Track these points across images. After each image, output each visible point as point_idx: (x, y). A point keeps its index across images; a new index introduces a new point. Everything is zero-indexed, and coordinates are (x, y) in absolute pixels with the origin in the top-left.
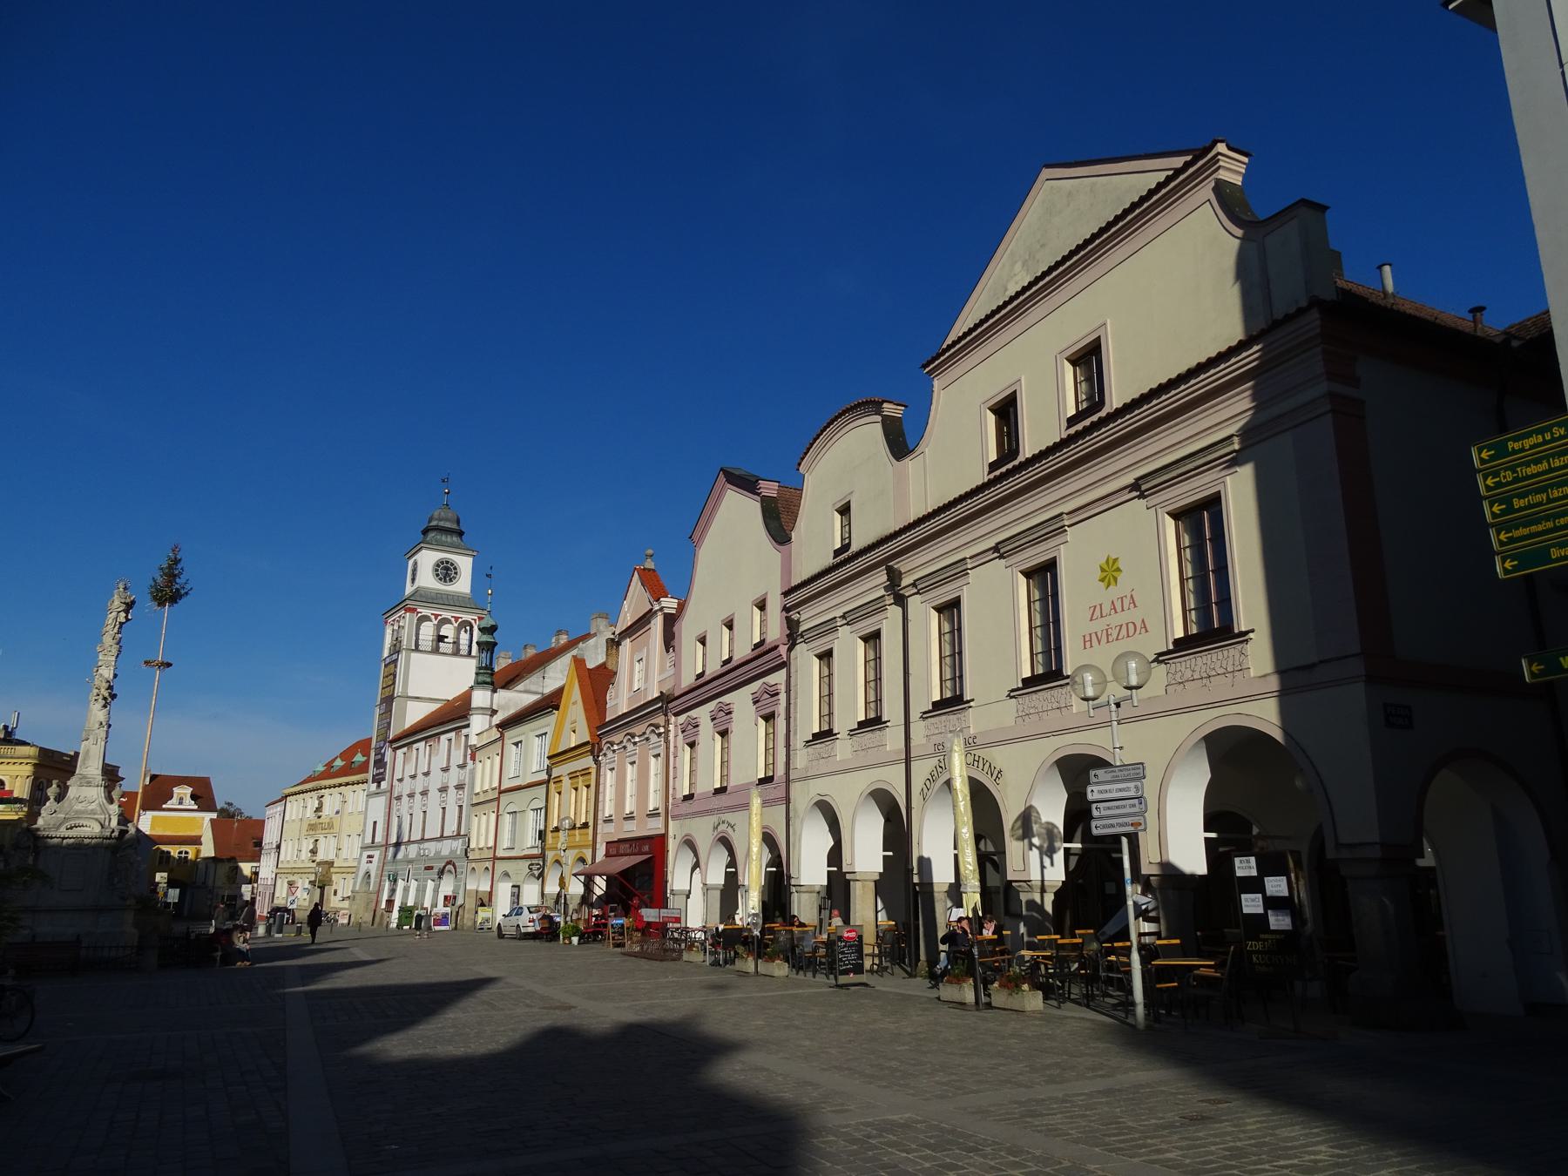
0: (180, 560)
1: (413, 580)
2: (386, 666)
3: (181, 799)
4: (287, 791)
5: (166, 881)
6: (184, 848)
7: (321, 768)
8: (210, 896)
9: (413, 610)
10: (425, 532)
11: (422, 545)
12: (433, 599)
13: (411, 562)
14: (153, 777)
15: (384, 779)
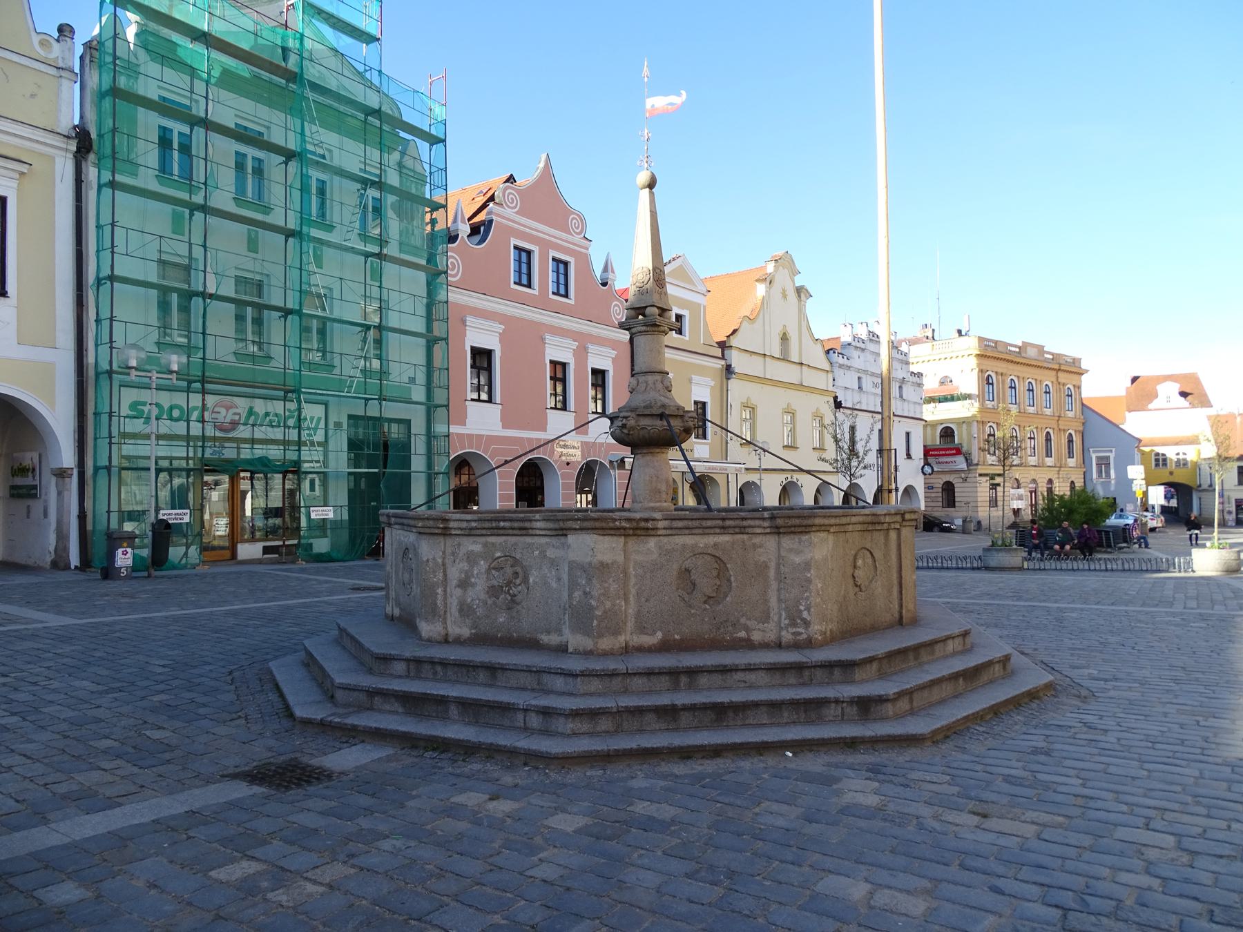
5: (1143, 476)
6: (1181, 449)
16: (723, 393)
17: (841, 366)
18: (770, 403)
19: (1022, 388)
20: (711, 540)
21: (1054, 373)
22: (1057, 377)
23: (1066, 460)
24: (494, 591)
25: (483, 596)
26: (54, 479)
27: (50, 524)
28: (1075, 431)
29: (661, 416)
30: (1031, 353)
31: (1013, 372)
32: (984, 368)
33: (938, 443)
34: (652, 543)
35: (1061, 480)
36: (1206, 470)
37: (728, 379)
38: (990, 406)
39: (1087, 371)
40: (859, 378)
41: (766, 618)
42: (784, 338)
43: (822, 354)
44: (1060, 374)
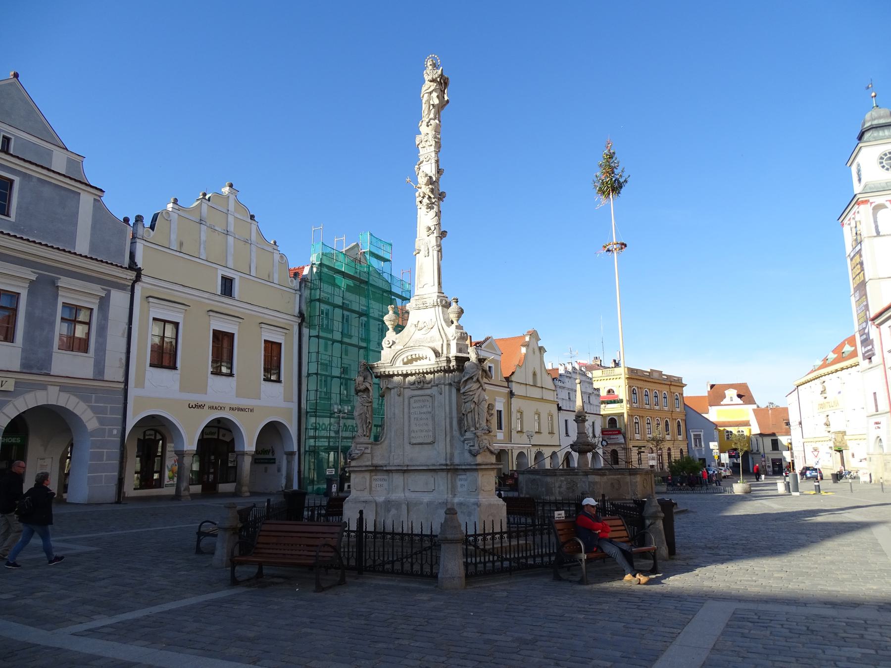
0: (614, 153)
1: (860, 180)
2: (852, 260)
3: (731, 398)
4: (798, 382)
5: (717, 448)
6: (741, 429)
7: (819, 363)
8: (763, 459)
9: (866, 202)
10: (860, 137)
11: (860, 145)
12: (884, 188)
13: (854, 169)
14: (712, 386)
15: (874, 354)
16: (509, 405)
17: (560, 387)
18: (529, 408)
19: (652, 395)
20: (617, 476)
21: (668, 387)
22: (670, 389)
23: (677, 436)
24: (568, 489)
25: (565, 490)
26: (285, 457)
27: (282, 475)
28: (681, 420)
29: (588, 445)
30: (656, 375)
31: (647, 387)
32: (631, 385)
33: (608, 427)
34: (605, 477)
35: (675, 448)
36: (754, 440)
37: (511, 398)
38: (635, 406)
39: (686, 385)
40: (569, 393)
41: (629, 494)
42: (534, 374)
43: (551, 380)
44: (672, 387)
